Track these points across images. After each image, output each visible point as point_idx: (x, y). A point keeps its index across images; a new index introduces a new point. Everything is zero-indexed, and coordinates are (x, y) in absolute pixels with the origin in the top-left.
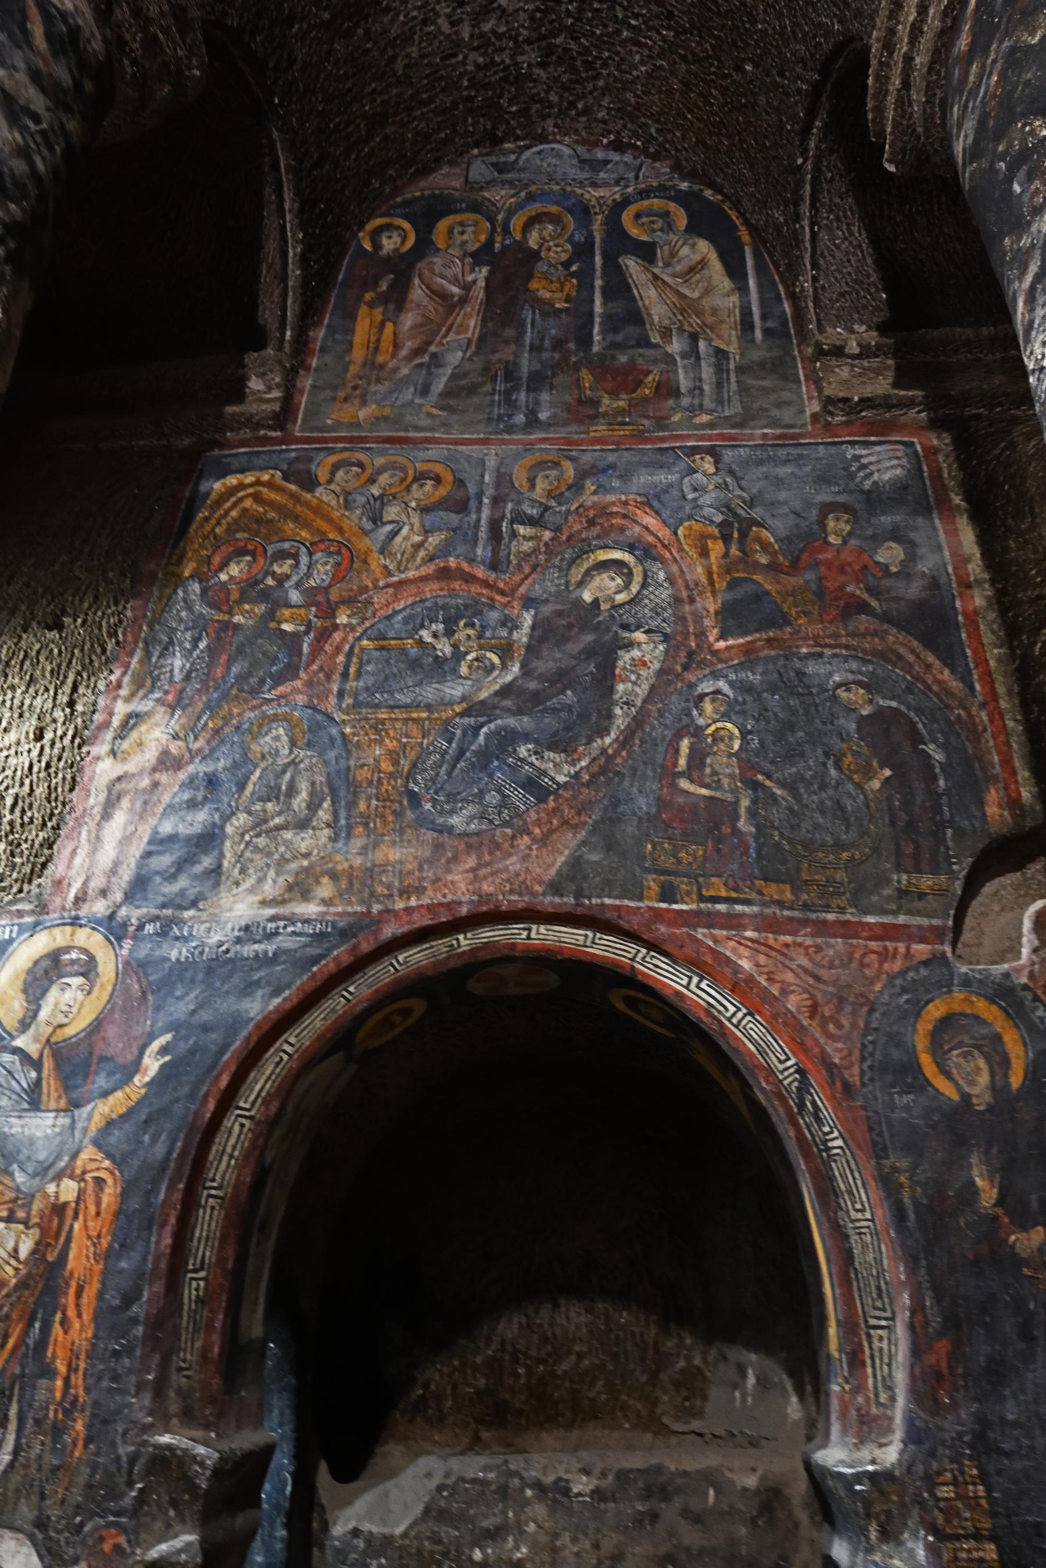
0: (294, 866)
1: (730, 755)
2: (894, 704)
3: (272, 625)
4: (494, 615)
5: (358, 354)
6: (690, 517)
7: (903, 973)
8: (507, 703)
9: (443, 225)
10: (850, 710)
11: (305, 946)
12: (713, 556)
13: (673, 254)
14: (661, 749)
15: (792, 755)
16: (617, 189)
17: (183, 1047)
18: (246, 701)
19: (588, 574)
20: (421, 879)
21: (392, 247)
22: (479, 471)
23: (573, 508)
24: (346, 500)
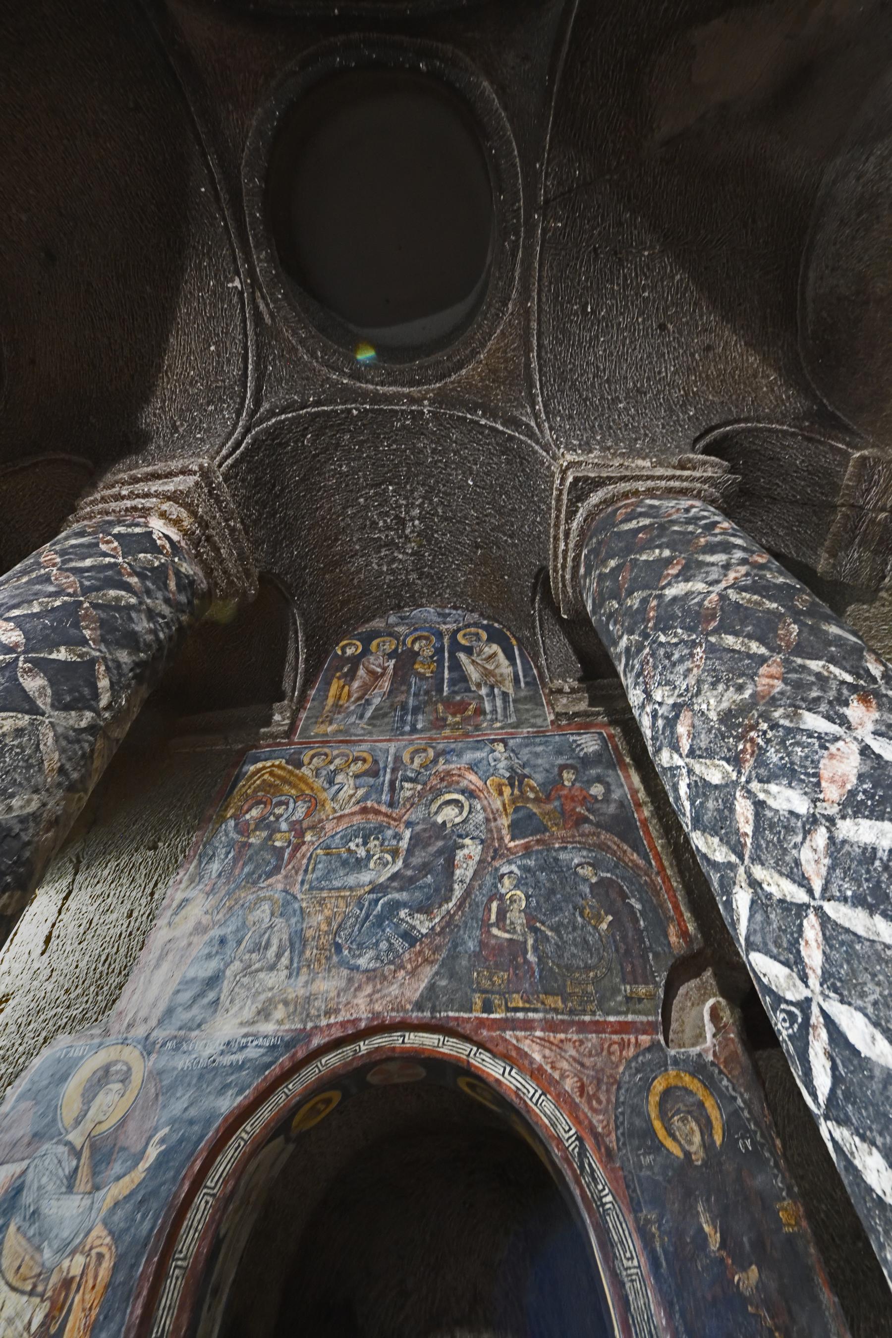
0: (263, 997)
1: (520, 911)
2: (609, 875)
3: (270, 843)
4: (389, 833)
5: (330, 701)
6: (493, 775)
7: (636, 1057)
8: (395, 884)
10: (585, 880)
11: (263, 1055)
12: (505, 794)
13: (481, 651)
14: (481, 909)
15: (555, 909)
17: (176, 1137)
18: (250, 888)
19: (440, 808)
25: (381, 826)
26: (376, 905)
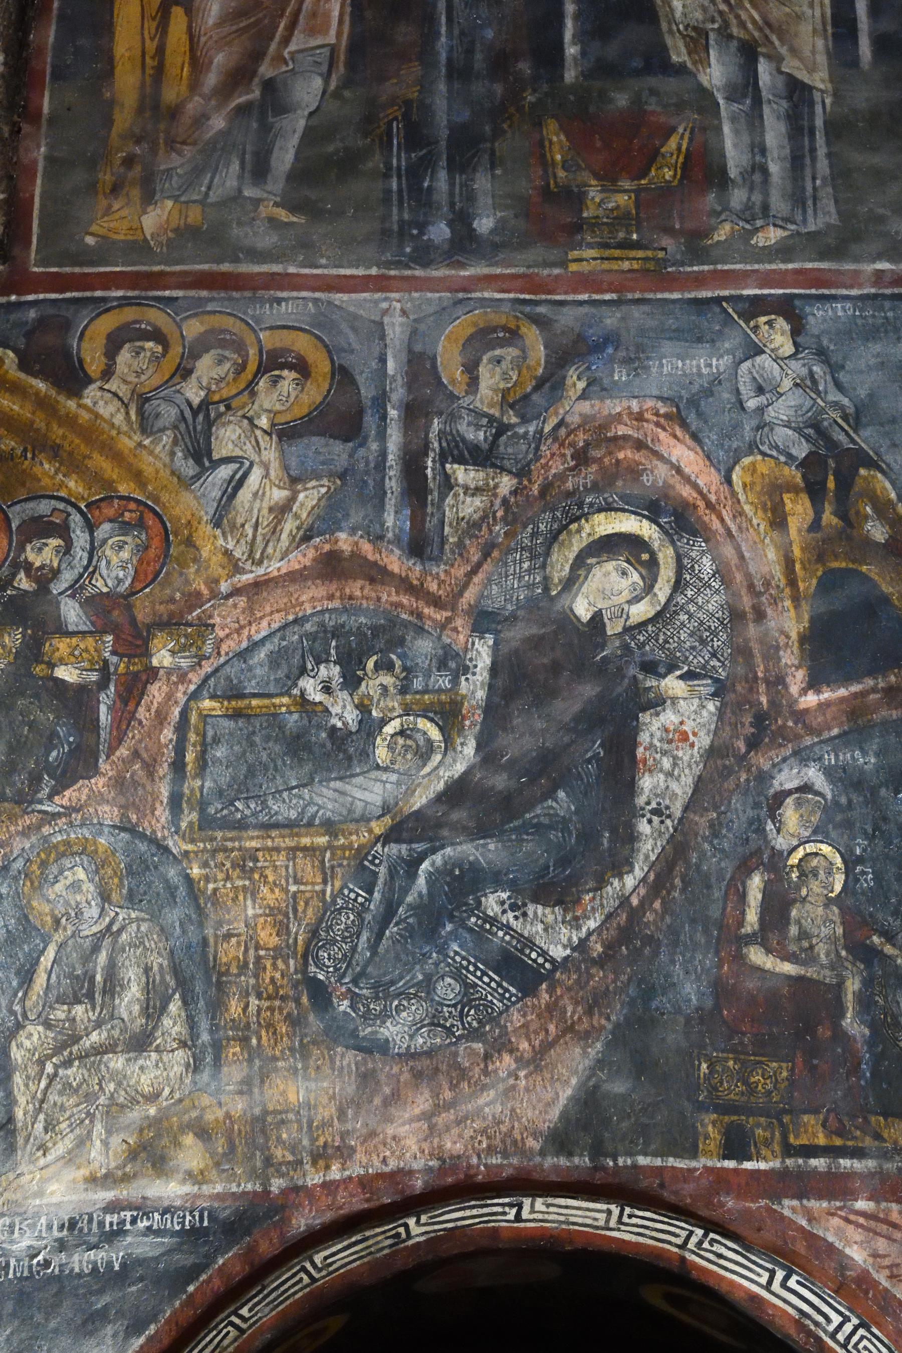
0: (134, 1115)
1: (829, 902)
3: (39, 670)
6: (752, 448)
19: (580, 562)
20: (344, 1135)
22: (376, 351)
23: (547, 429)
24: (140, 412)
25: (393, 622)
26: (412, 875)
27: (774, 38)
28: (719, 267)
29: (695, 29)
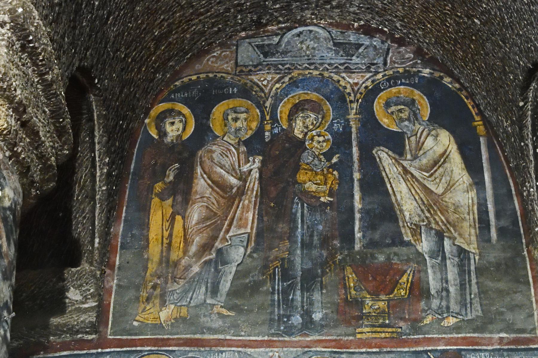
9: (218, 111)
13: (419, 146)
16: (368, 75)
21: (176, 133)
27: (452, 229)
28: (426, 336)
29: (415, 225)
